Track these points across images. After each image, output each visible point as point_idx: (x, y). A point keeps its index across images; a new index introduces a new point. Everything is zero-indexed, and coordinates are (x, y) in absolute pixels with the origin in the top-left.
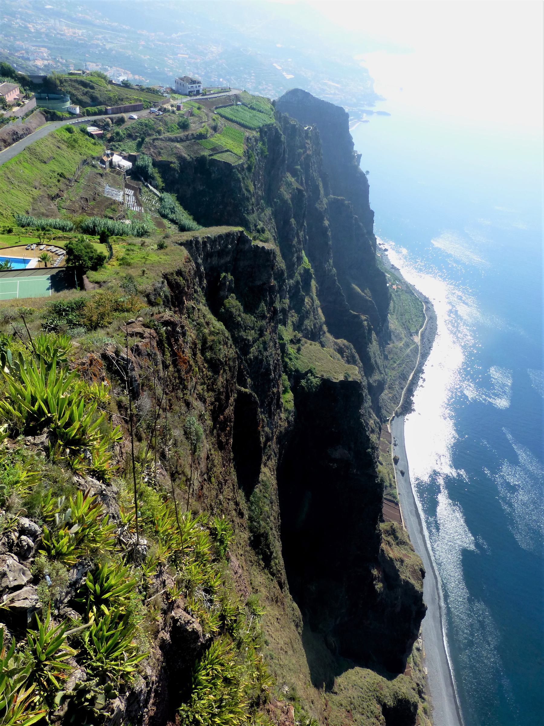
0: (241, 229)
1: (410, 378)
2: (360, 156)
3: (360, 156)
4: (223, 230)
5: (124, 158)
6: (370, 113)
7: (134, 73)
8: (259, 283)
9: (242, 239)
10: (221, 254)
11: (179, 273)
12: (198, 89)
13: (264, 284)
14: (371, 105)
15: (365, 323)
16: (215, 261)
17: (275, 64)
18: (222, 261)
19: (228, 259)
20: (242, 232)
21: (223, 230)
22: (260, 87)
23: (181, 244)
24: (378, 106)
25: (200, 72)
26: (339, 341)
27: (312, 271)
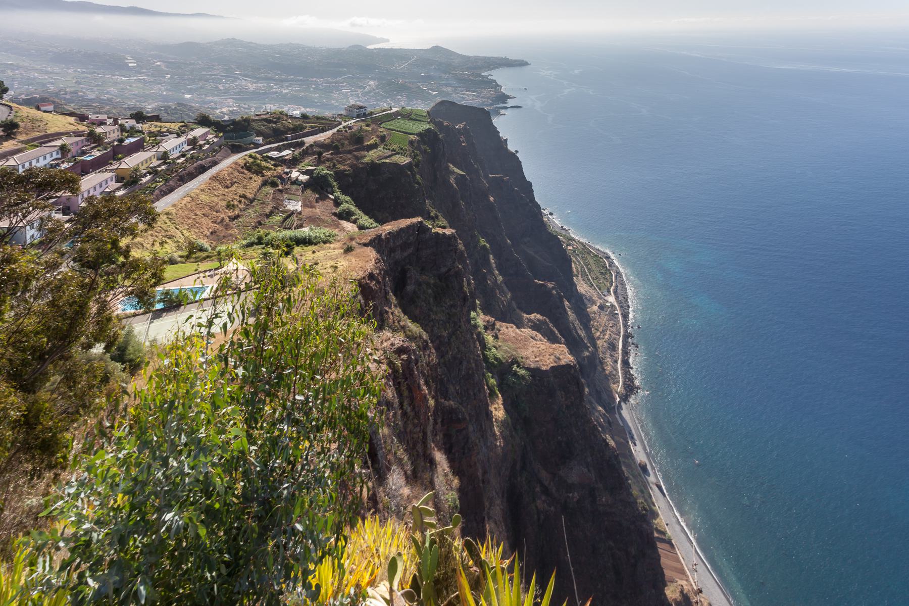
0: (420, 219)
1: (620, 346)
4: (404, 223)
6: (506, 108)
8: (444, 270)
9: (421, 228)
10: (405, 246)
11: (371, 276)
13: (449, 270)
15: (554, 292)
16: (398, 255)
18: (406, 254)
19: (410, 250)
20: (421, 222)
21: (404, 223)
23: (365, 245)
24: (511, 103)
26: (532, 316)
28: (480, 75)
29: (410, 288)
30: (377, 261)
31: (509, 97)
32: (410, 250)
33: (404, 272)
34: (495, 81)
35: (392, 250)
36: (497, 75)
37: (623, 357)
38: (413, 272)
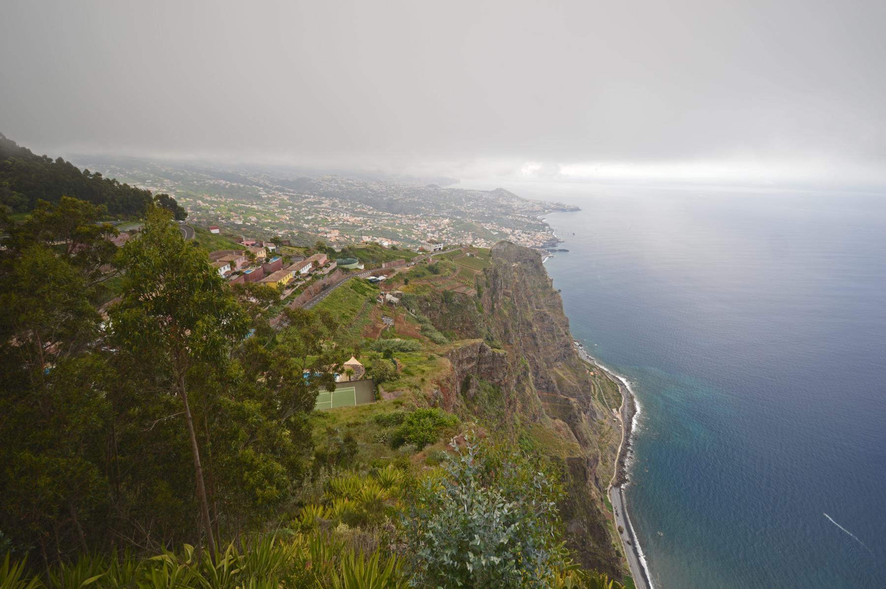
0: (481, 340)
2: (552, 281)
3: (552, 281)
5: (394, 295)
6: (555, 251)
7: (392, 239)
8: (496, 380)
10: (470, 360)
14: (554, 245)
16: (466, 366)
18: (470, 366)
24: (559, 246)
27: (528, 365)
28: (534, 219)
29: (472, 391)
30: (453, 369)
31: (558, 241)
32: (474, 364)
33: (468, 379)
34: (547, 225)
35: (460, 362)
36: (549, 219)
37: (620, 457)
38: (474, 380)
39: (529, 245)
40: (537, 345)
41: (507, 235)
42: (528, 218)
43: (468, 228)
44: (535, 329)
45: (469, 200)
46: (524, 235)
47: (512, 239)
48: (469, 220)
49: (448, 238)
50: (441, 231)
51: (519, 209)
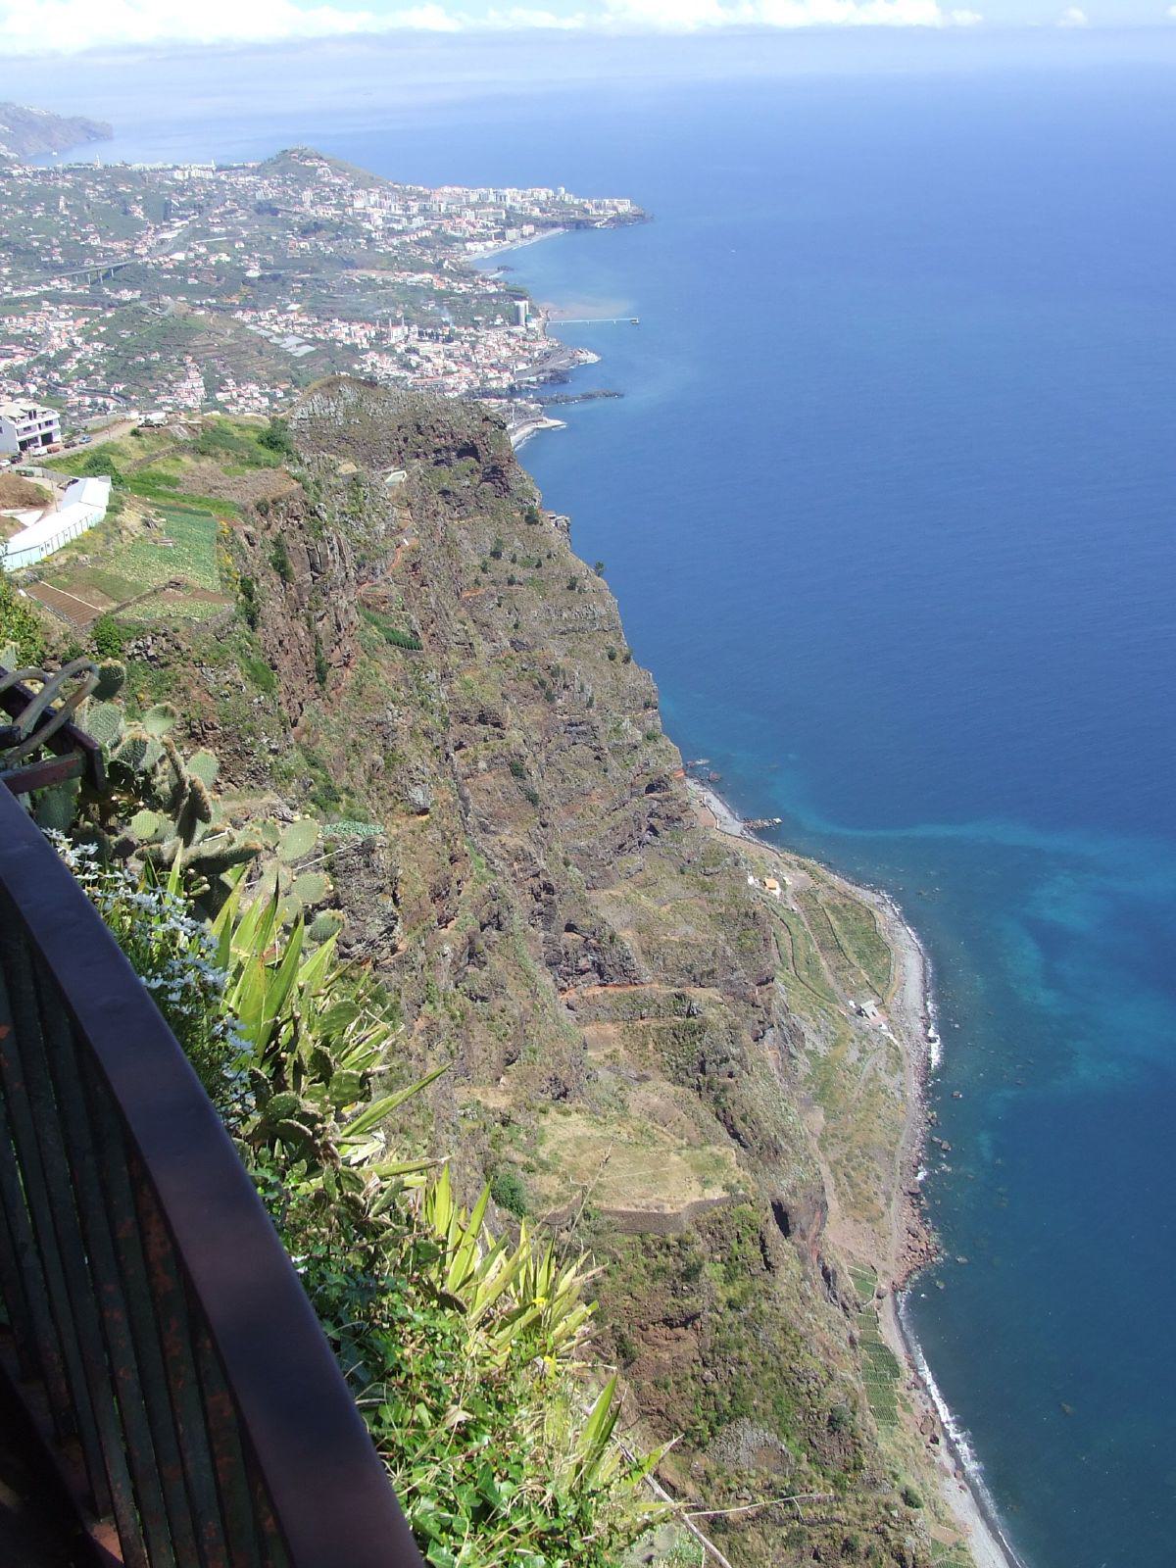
12: (46, 430)
17: (251, 327)
22: (220, 396)
25: (33, 389)
39: (460, 382)
40: (533, 799)
41: (353, 351)
42: (437, 268)
43: (175, 337)
44: (515, 735)
45: (164, 213)
46: (427, 347)
47: (385, 367)
48: (173, 304)
49: (94, 393)
50: (51, 364)
51: (392, 232)
